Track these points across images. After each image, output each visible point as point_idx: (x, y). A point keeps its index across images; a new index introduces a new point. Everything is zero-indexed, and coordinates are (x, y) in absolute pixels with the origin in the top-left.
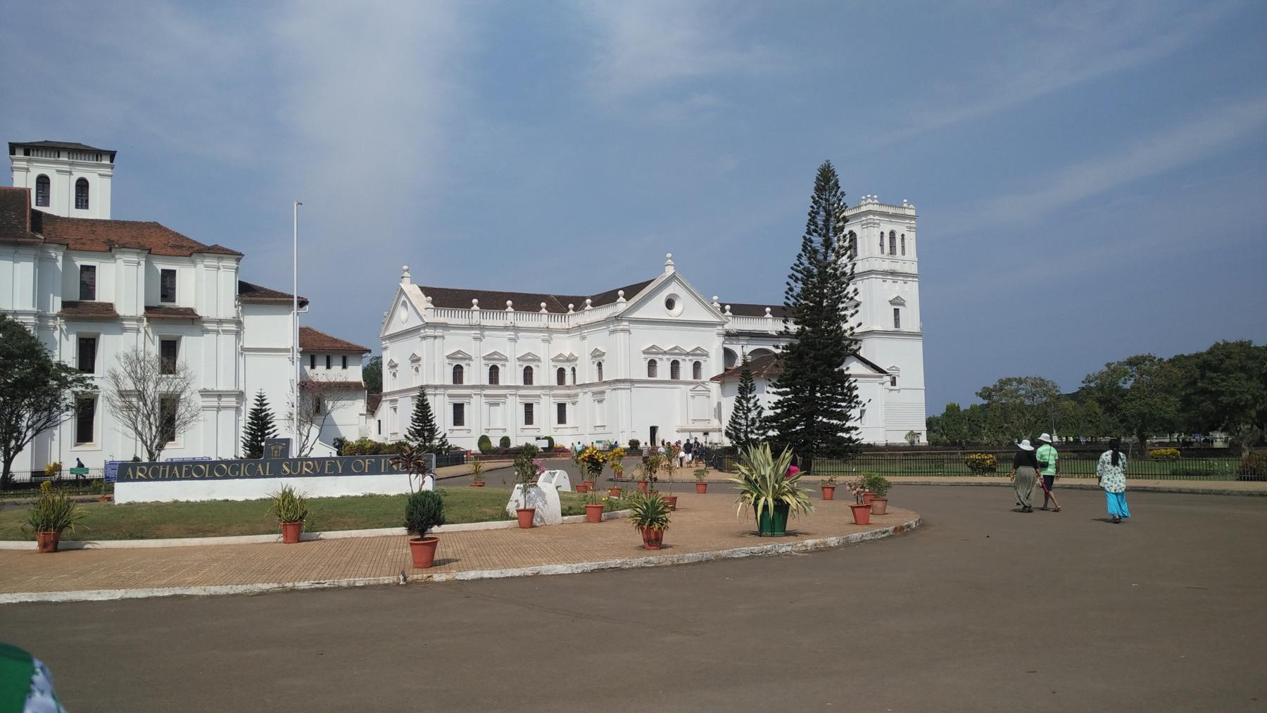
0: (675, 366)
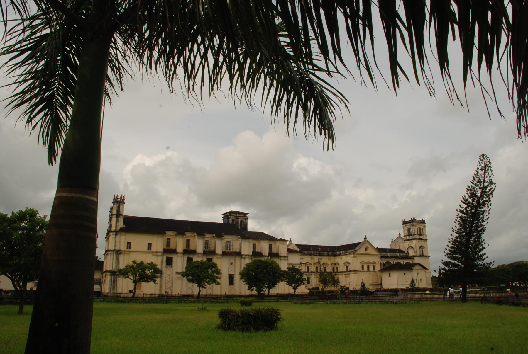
0: (368, 266)
